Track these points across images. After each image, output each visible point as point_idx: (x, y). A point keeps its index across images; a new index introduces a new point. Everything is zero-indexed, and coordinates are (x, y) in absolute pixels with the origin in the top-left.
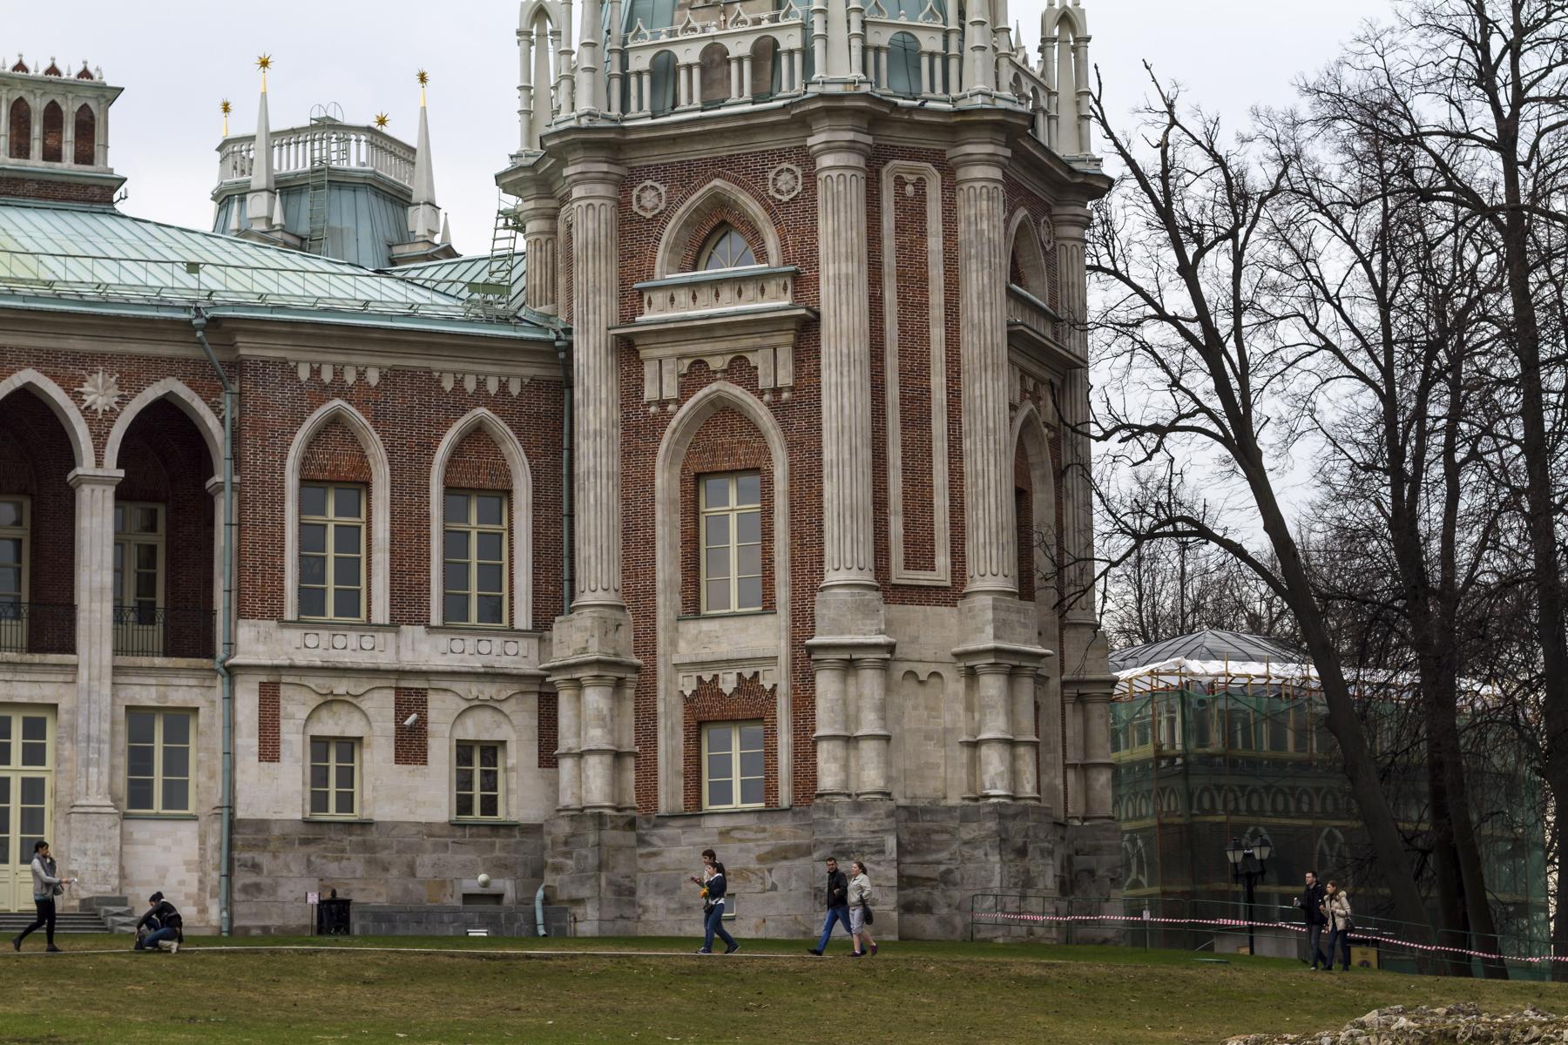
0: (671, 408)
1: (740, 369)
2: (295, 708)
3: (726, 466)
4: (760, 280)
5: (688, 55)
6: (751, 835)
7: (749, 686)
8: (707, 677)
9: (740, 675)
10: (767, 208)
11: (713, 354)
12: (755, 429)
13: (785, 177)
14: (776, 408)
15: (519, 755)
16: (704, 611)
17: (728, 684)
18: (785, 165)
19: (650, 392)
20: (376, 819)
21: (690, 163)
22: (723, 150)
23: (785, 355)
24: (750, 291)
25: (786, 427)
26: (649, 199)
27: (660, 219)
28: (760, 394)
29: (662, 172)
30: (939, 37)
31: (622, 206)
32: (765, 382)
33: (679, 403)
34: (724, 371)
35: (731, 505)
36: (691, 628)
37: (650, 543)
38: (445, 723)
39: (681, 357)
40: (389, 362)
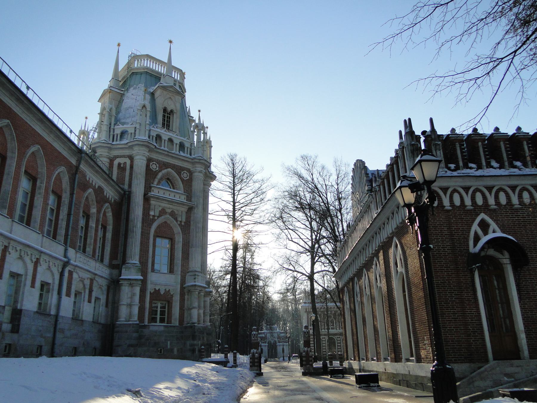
0: (156, 218)
8: (157, 289)
13: (185, 174)
14: (180, 225)
28: (177, 221)
31: (148, 166)
32: (180, 219)
33: (158, 217)
35: (163, 245)
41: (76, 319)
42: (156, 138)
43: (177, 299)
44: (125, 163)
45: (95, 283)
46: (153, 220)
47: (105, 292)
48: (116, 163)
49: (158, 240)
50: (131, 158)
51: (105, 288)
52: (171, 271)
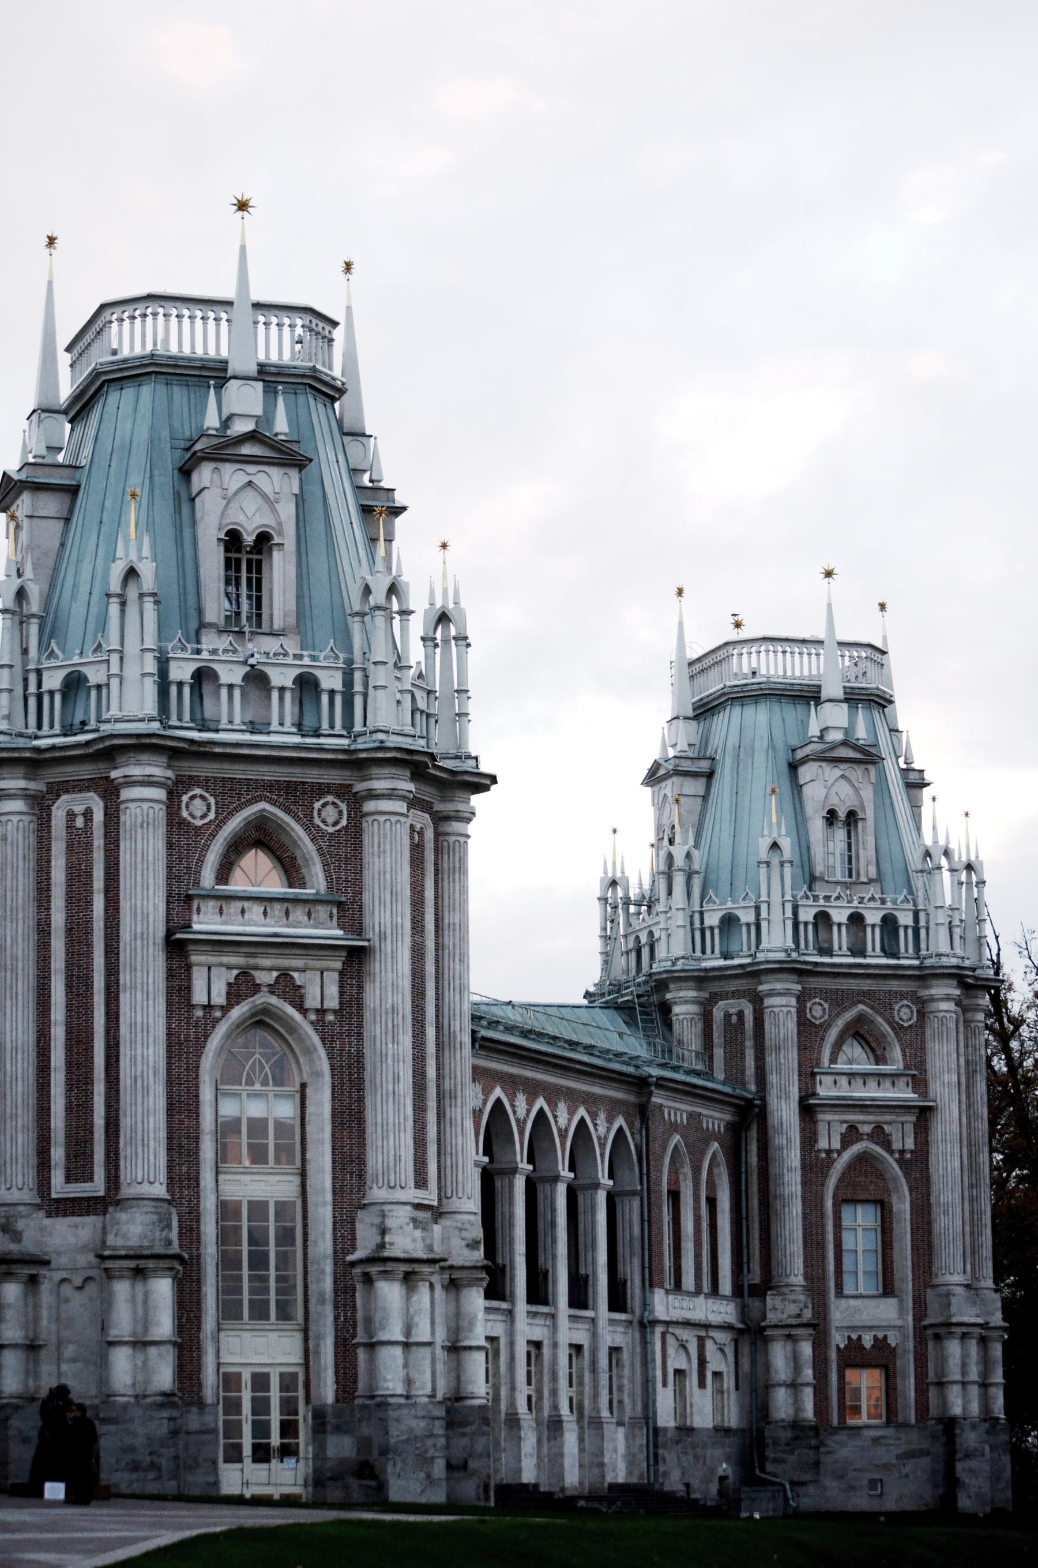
1: (880, 1135)
2: (671, 1351)
3: (862, 1197)
4: (894, 1077)
5: (839, 916)
6: (892, 1441)
7: (881, 1344)
8: (854, 1336)
9: (875, 1336)
10: (893, 1029)
11: (864, 1123)
12: (881, 1175)
14: (901, 1162)
15: (729, 1382)
16: (845, 1292)
17: (868, 1341)
18: (905, 1002)
19: (823, 1144)
20: (695, 1425)
21: (842, 991)
22: (867, 985)
23: (909, 1129)
24: (887, 1083)
25: (907, 1175)
26: (817, 1011)
27: (826, 1026)
28: (891, 1152)
29: (827, 995)
30: (911, 915)
31: (801, 1012)
32: (897, 1145)
34: (868, 1135)
35: (861, 1220)
36: (843, 1303)
37: (821, 1245)
38: (716, 1362)
39: (845, 1122)
40: (690, 1108)
41: (685, 1430)
42: (816, 925)
43: (907, 1363)
44: (740, 1014)
45: (710, 1346)
46: (828, 1163)
47: (731, 1358)
48: (718, 1014)
49: (847, 1211)
50: (757, 1000)
51: (729, 1351)
52: (888, 1290)
